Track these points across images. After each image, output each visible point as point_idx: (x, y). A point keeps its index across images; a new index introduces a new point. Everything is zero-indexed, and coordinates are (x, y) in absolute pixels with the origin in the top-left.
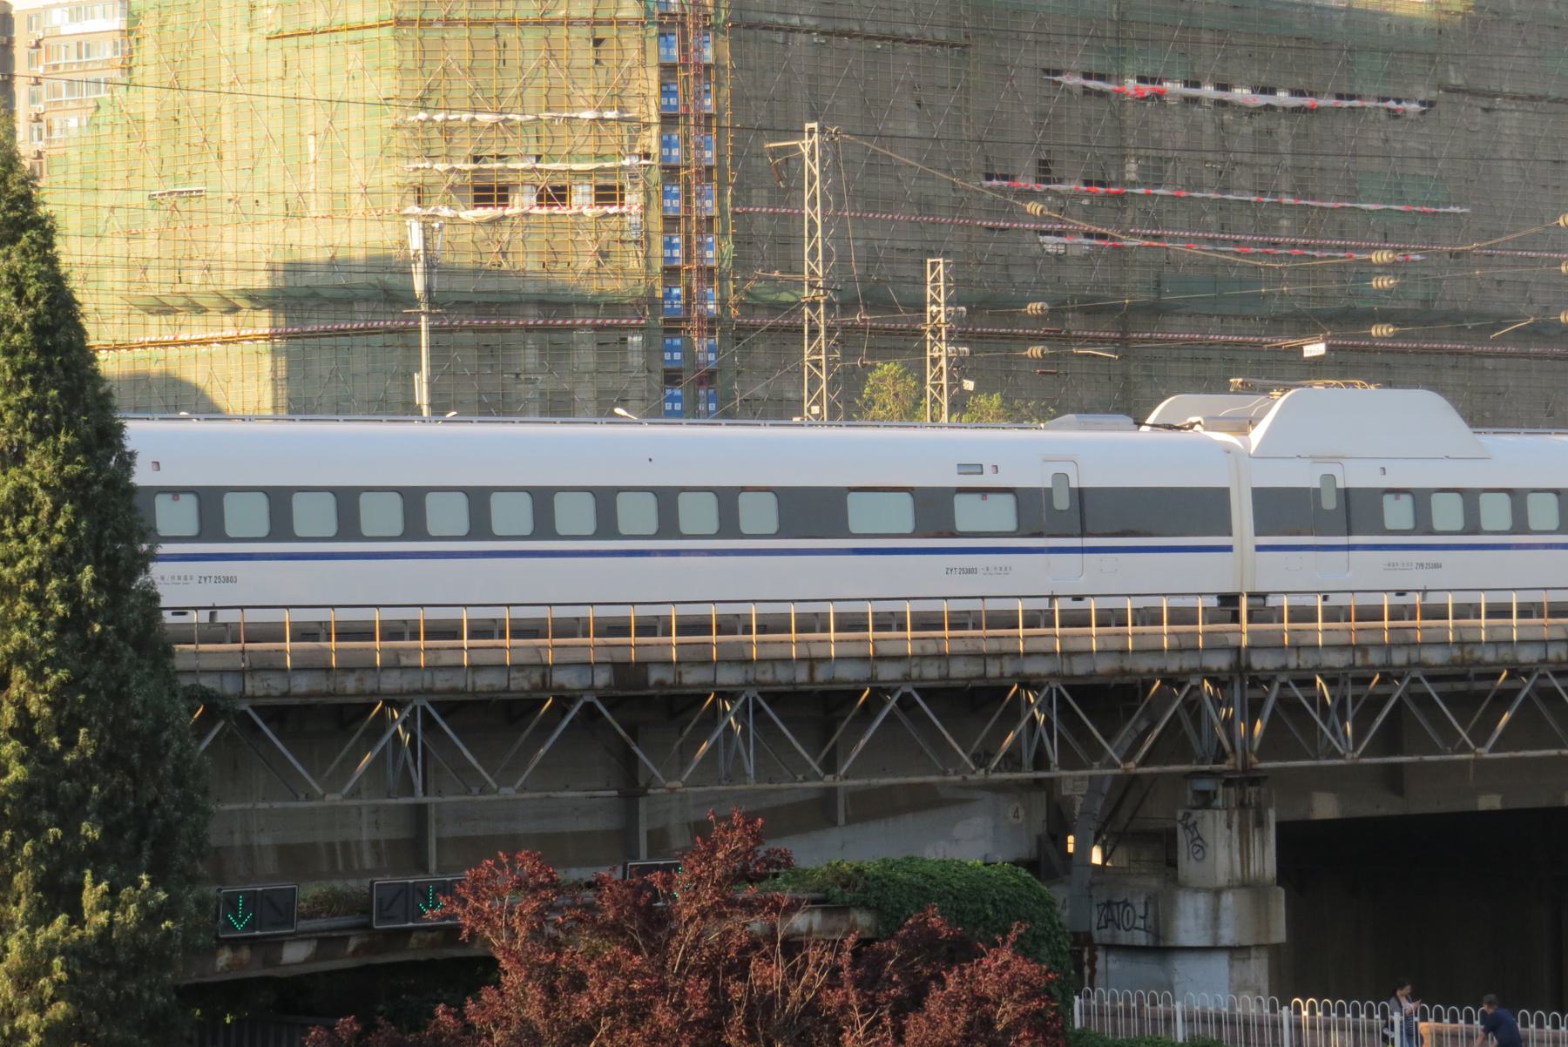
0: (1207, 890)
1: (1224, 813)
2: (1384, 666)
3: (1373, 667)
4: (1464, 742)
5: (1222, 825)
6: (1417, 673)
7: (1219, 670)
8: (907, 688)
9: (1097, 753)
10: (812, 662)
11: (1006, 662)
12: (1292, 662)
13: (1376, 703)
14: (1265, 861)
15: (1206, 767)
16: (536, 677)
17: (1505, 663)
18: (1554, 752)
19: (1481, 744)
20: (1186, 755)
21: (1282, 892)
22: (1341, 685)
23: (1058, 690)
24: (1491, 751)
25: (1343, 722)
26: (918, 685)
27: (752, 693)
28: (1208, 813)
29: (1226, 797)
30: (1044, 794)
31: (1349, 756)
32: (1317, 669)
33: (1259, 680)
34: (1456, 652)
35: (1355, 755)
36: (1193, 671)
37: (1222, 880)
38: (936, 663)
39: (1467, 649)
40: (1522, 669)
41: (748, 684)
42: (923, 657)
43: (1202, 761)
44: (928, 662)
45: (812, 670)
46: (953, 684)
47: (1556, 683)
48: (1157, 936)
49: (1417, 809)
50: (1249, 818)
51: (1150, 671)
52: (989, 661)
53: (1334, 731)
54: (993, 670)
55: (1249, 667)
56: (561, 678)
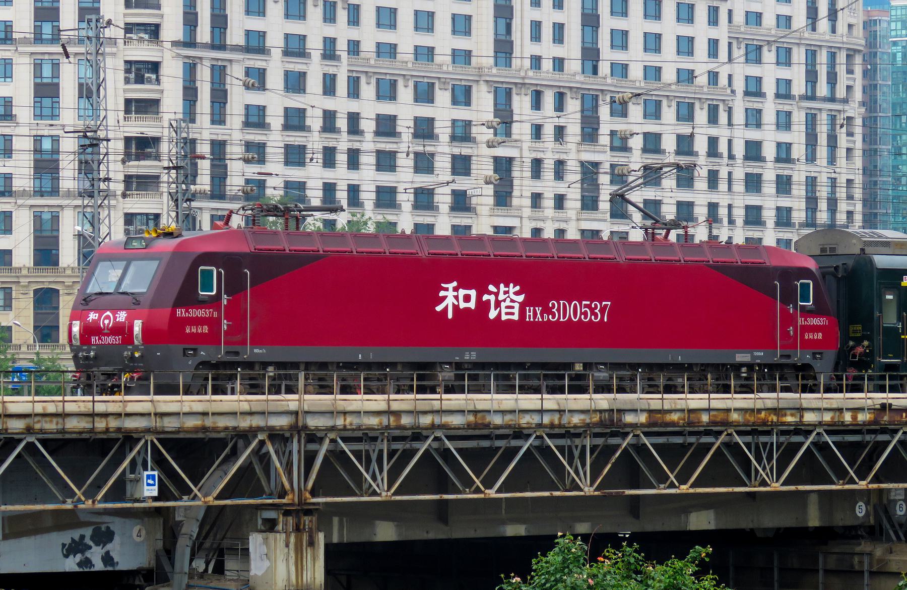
1: (284, 535)
2: (412, 428)
3: (403, 428)
4: (478, 486)
6: (439, 434)
7: (282, 428)
8: (31, 439)
9: (187, 491)
11: (110, 419)
12: (340, 422)
13: (408, 455)
15: (270, 501)
17: (508, 426)
18: (547, 494)
19: (491, 488)
20: (258, 492)
22: (379, 440)
23: (152, 441)
24: (499, 491)
25: (381, 471)
26: (40, 436)
28: (271, 536)
29: (286, 524)
30: (162, 521)
31: (384, 494)
32: (359, 428)
33: (313, 437)
34: (471, 418)
35: (389, 494)
36: (260, 429)
38: (55, 420)
39: (479, 415)
40: (526, 432)
42: (44, 415)
43: (271, 495)
44: (48, 419)
46: (67, 436)
47: (549, 442)
49: (458, 534)
50: (303, 542)
51: (226, 428)
52: (97, 419)
53: (374, 478)
54: (100, 425)
55: (305, 427)
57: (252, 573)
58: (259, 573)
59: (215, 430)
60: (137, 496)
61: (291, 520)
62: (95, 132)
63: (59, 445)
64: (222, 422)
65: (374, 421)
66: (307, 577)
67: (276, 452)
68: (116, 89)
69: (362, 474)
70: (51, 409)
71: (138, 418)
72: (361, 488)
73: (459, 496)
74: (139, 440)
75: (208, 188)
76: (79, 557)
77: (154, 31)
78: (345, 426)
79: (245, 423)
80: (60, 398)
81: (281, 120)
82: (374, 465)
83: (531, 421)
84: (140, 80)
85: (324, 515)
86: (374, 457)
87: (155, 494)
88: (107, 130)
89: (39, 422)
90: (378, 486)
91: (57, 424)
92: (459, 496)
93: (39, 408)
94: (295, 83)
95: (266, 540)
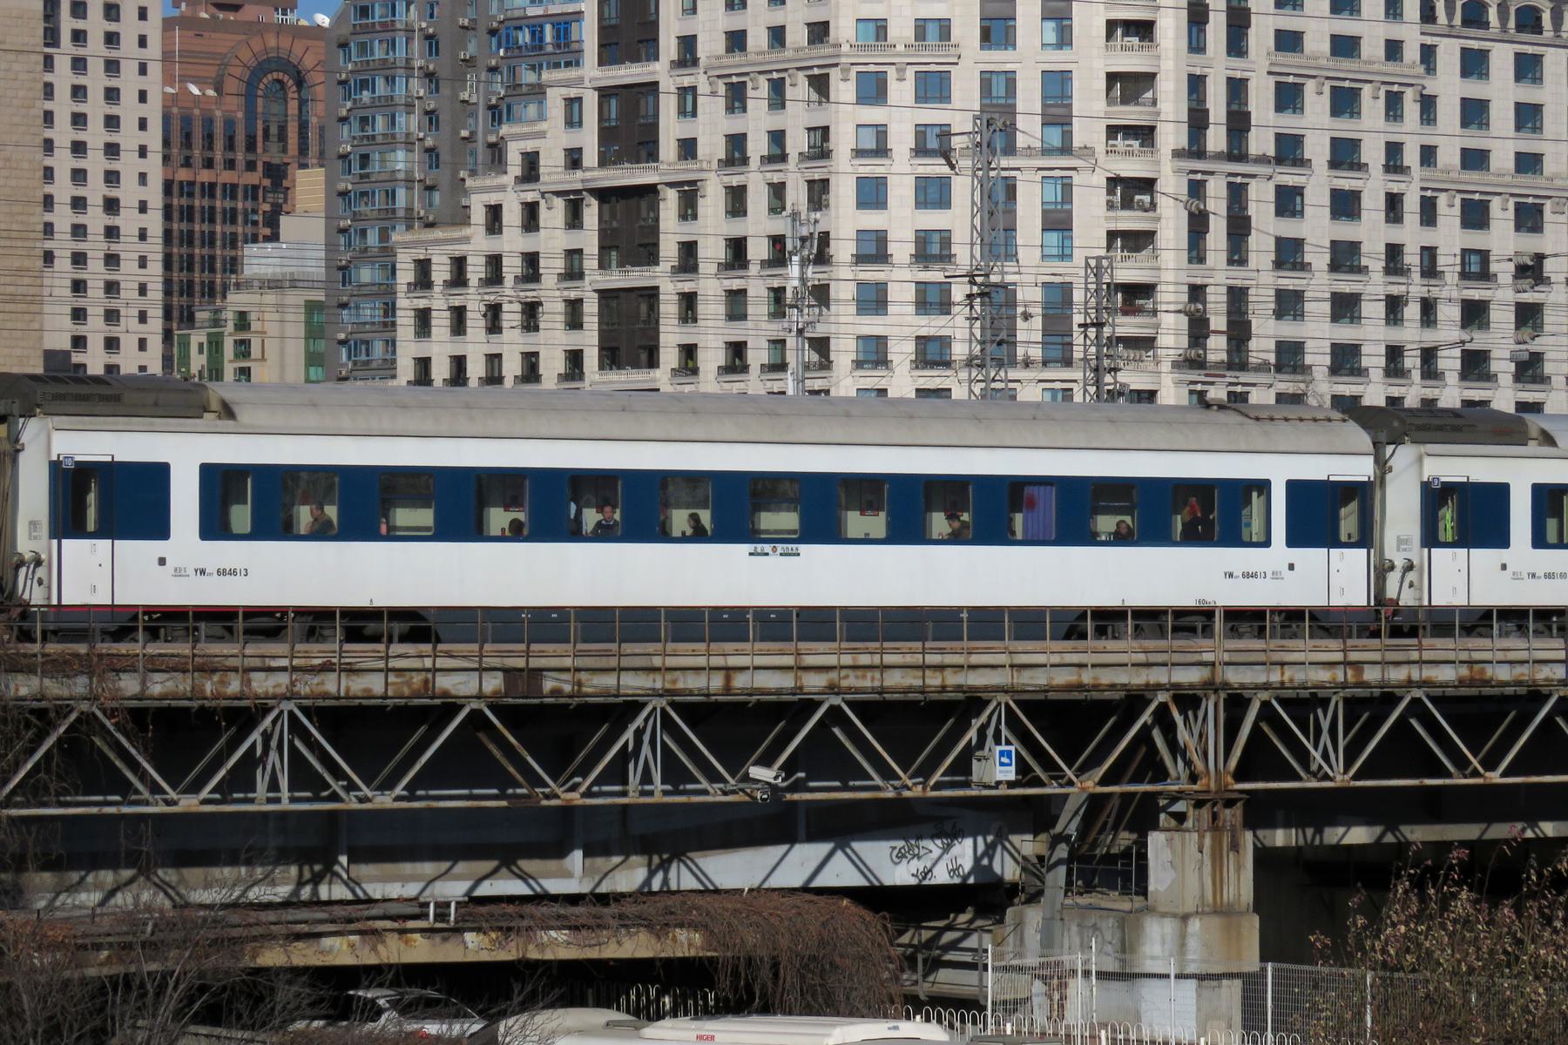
0: (1174, 916)
5: (1194, 848)
6: (1417, 693)
7: (1192, 686)
8: (836, 700)
10: (729, 671)
11: (948, 672)
12: (1275, 677)
14: (1242, 884)
16: (417, 679)
17: (1518, 683)
21: (1256, 919)
23: (1007, 705)
24: (1504, 775)
27: (662, 702)
28: (1176, 835)
31: (1339, 778)
34: (1464, 671)
35: (1347, 777)
36: (1159, 687)
37: (1190, 906)
38: (869, 675)
39: (1477, 667)
40: (1545, 690)
41: (656, 693)
44: (859, 673)
45: (728, 679)
48: (1123, 961)
51: (1112, 687)
52: (928, 672)
53: (1325, 756)
54: (934, 680)
55: (1226, 685)
56: (444, 682)
57: (1151, 888)
58: (1161, 888)
59: (1096, 687)
60: (986, 780)
61: (1205, 813)
62: (987, 275)
63: (878, 711)
64: (1107, 677)
65: (1323, 675)
66: (1229, 894)
67: (1186, 719)
68: (1093, 216)
69: (1308, 752)
70: (865, 659)
71: (987, 671)
72: (1306, 767)
73: (1448, 781)
74: (988, 702)
75: (1224, 356)
76: (917, 865)
77: (1145, 134)
78: (1282, 683)
79: (1139, 678)
80: (877, 645)
81: (1327, 258)
82: (1325, 738)
83: (1551, 676)
84: (1127, 204)
85: (1260, 812)
86: (1325, 725)
87: (1012, 776)
88: (1003, 273)
89: (847, 677)
90: (1331, 767)
91: (873, 679)
92: (1448, 781)
93: (847, 660)
94: (1345, 205)
95: (1170, 841)
